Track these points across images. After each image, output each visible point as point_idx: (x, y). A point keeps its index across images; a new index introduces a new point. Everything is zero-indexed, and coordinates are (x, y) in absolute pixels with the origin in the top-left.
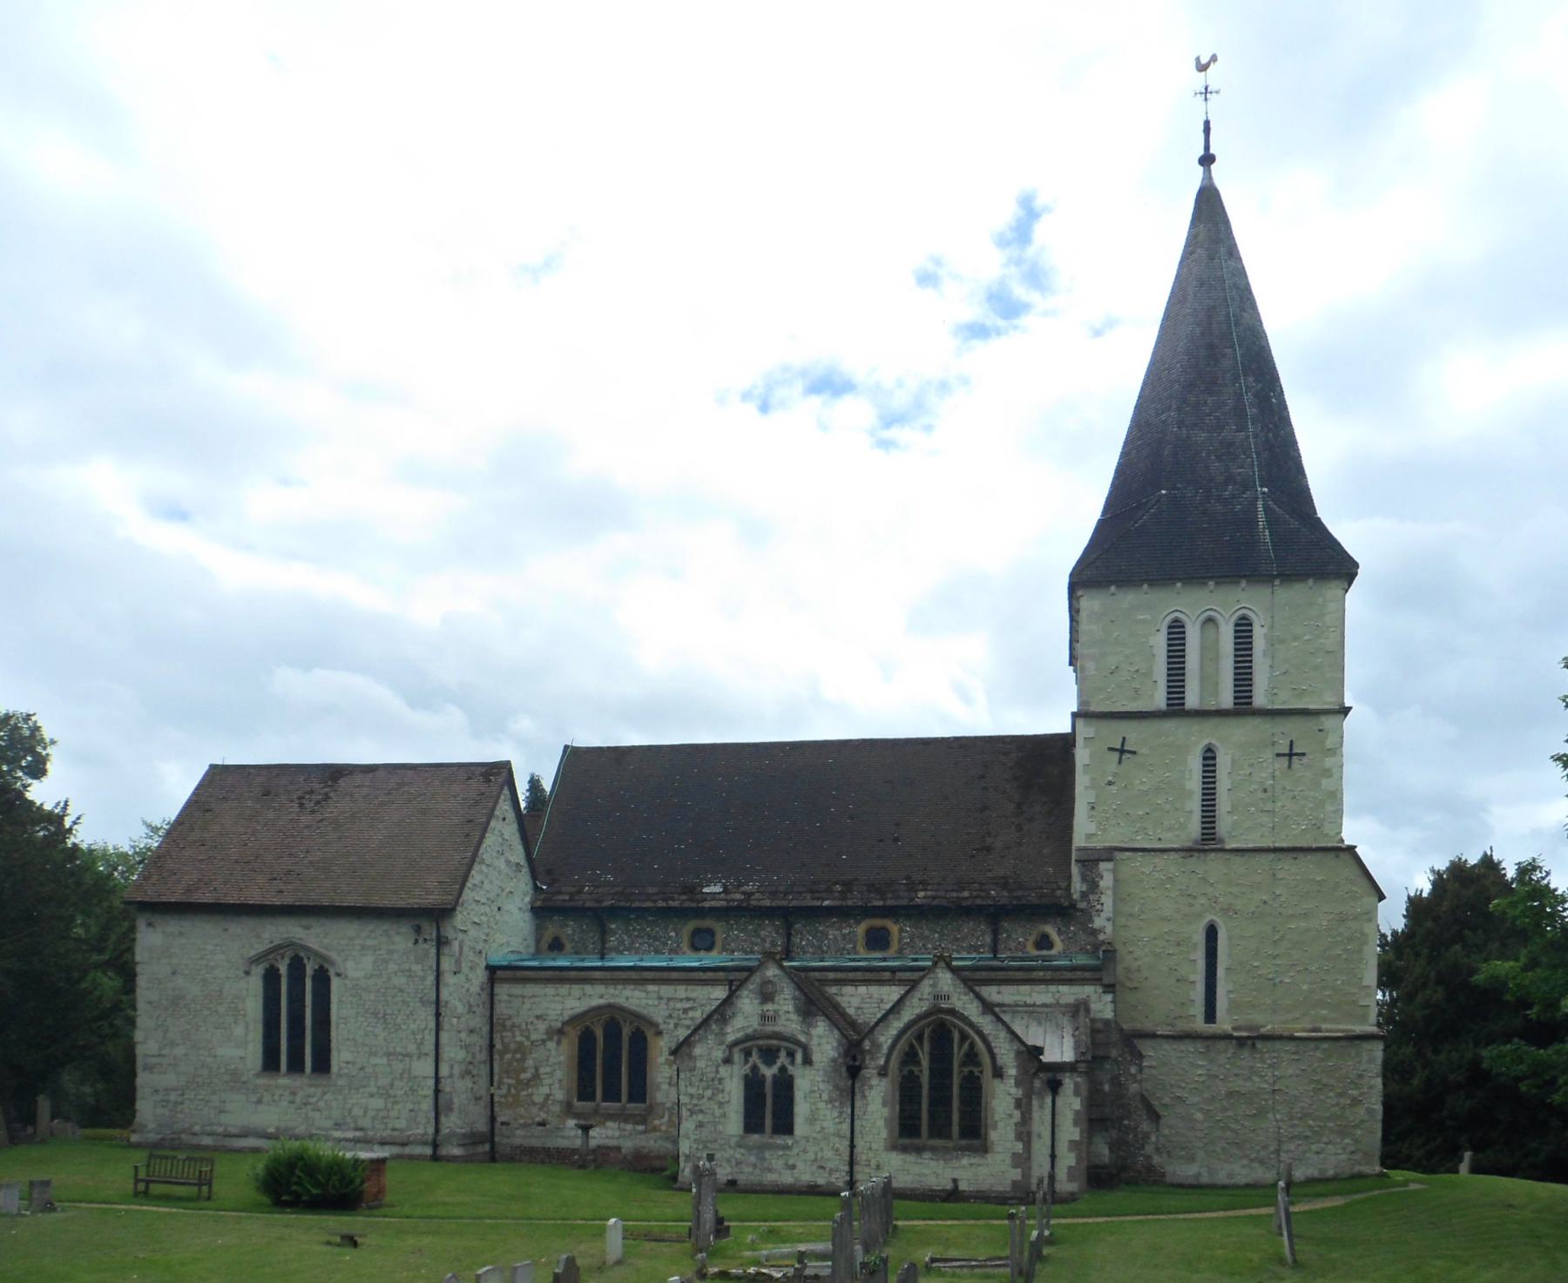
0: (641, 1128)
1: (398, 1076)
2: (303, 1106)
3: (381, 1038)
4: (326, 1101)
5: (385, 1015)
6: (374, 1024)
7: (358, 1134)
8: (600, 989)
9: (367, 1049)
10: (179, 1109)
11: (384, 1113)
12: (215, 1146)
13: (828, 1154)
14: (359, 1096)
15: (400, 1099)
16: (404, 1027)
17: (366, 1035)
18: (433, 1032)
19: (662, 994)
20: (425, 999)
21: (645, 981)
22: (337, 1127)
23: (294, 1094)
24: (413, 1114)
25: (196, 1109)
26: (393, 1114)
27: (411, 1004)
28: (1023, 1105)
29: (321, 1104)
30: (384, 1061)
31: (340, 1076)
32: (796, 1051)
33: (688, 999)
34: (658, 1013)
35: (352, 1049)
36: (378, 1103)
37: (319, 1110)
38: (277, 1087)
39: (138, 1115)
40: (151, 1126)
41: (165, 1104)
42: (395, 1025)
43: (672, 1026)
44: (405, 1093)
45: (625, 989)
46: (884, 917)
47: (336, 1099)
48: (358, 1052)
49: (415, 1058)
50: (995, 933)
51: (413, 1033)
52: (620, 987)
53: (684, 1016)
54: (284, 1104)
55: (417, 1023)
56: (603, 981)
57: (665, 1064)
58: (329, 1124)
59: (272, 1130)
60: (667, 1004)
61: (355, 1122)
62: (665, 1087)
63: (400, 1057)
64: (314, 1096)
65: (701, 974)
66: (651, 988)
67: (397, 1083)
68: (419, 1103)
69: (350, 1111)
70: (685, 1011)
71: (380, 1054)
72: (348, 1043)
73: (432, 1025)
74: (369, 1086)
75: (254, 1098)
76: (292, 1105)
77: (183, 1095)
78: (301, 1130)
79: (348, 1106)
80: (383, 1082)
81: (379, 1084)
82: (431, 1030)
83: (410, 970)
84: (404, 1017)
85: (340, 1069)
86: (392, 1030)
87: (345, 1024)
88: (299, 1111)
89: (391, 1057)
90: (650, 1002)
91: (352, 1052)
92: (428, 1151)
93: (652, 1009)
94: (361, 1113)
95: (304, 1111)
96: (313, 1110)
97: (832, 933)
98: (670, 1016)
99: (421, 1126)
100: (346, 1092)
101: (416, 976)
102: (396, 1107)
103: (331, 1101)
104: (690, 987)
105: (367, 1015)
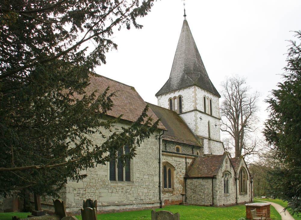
0: (172, 194)
2: (125, 193)
3: (146, 169)
4: (132, 191)
5: (147, 162)
8: (165, 157)
9: (143, 173)
10: (84, 197)
11: (147, 194)
13: (233, 197)
14: (141, 188)
15: (151, 189)
16: (151, 166)
17: (142, 168)
18: (158, 168)
19: (175, 160)
20: (156, 157)
21: (173, 156)
22: (136, 200)
23: (123, 189)
25: (90, 196)
26: (149, 194)
27: (153, 159)
28: (249, 185)
29: (131, 192)
30: (147, 177)
31: (136, 182)
32: (229, 174)
33: (179, 161)
34: (174, 164)
35: (139, 173)
37: (130, 194)
38: (118, 186)
40: (74, 204)
41: (78, 194)
42: (150, 165)
46: (179, 145)
47: (135, 190)
49: (154, 176)
50: (193, 151)
51: (154, 168)
52: (168, 157)
53: (179, 166)
54: (120, 193)
55: (155, 165)
56: (166, 155)
58: (133, 199)
59: (116, 202)
61: (140, 198)
62: (176, 183)
64: (129, 189)
66: (173, 158)
67: (151, 184)
68: (155, 190)
69: (139, 194)
70: (179, 164)
72: (138, 171)
73: (158, 166)
74: (143, 185)
75: (110, 191)
79: (138, 192)
80: (147, 184)
81: (146, 185)
83: (152, 148)
88: (124, 195)
90: (173, 161)
92: (159, 205)
93: (173, 163)
96: (129, 194)
98: (177, 166)
99: (156, 197)
100: (138, 187)
101: (154, 150)
102: (150, 192)
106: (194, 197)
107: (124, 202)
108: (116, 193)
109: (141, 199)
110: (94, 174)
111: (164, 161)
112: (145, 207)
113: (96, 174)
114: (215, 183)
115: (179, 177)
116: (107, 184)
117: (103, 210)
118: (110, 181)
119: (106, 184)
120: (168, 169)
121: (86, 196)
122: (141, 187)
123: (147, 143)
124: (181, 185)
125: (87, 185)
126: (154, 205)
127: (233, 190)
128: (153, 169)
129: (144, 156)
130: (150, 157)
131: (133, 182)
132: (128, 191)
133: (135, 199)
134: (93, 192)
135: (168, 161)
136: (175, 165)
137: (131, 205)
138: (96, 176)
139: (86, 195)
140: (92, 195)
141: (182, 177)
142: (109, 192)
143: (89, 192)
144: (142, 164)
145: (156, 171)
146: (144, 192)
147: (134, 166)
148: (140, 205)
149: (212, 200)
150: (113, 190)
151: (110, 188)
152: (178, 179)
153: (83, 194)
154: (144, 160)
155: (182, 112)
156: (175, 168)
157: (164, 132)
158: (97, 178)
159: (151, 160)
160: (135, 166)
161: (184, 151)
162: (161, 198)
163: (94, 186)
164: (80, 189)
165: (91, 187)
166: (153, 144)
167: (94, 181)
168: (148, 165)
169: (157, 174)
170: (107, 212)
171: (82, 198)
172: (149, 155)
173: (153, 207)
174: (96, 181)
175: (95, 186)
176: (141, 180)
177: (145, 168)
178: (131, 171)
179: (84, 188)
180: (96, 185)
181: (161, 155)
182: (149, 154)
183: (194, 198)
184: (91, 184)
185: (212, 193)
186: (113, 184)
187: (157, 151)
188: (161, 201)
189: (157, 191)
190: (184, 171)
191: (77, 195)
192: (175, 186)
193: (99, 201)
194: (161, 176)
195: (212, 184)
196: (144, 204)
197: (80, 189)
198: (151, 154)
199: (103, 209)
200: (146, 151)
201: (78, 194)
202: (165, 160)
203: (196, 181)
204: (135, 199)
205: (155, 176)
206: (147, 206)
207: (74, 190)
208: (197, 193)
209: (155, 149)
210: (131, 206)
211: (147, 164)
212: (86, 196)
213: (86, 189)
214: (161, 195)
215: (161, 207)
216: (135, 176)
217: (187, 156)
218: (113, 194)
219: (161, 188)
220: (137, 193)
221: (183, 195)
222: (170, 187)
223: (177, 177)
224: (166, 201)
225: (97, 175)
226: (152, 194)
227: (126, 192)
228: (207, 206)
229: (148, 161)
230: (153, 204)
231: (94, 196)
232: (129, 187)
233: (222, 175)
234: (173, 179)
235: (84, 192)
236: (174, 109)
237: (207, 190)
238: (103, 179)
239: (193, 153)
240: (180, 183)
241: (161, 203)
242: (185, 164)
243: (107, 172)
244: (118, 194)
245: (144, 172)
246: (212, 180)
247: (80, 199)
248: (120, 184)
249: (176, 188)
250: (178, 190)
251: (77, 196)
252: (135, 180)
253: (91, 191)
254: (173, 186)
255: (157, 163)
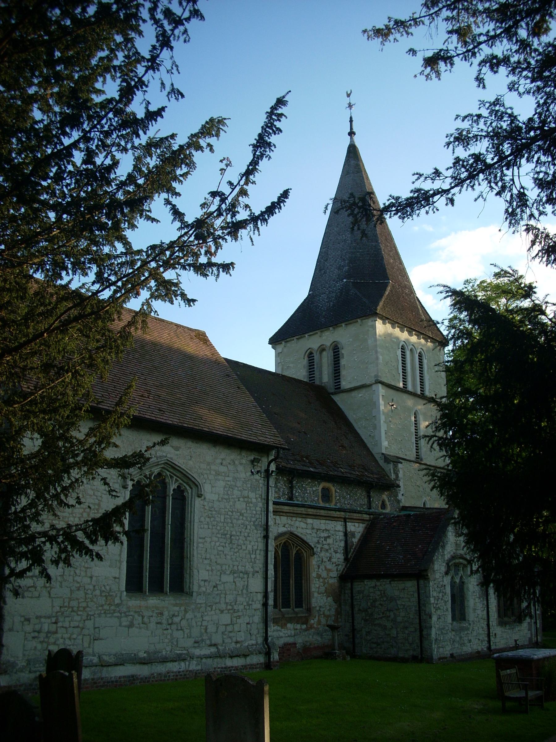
1: (240, 592)
2: (168, 627)
3: (228, 557)
4: (187, 620)
5: (231, 536)
6: (223, 544)
7: (213, 650)
8: (284, 519)
9: (219, 567)
10: (52, 640)
11: (230, 628)
12: (93, 679)
14: (213, 612)
15: (240, 614)
16: (244, 547)
18: (262, 553)
21: (308, 515)
22: (196, 645)
23: (161, 614)
24: (249, 626)
25: (70, 639)
26: (236, 628)
27: (249, 527)
29: (184, 623)
30: (230, 578)
31: (199, 594)
33: (326, 530)
34: (311, 539)
36: (226, 618)
37: (181, 630)
38: (147, 608)
39: (4, 651)
40: (21, 663)
41: (36, 634)
43: (319, 550)
44: (245, 609)
45: (296, 520)
47: (195, 616)
48: (212, 570)
49: (251, 575)
50: (369, 497)
51: (250, 553)
52: (294, 519)
53: (325, 542)
54: (152, 626)
55: (253, 543)
56: (286, 514)
57: (317, 577)
58: (189, 643)
59: (142, 655)
60: (316, 533)
61: (210, 639)
63: (241, 575)
65: (334, 512)
66: (310, 521)
67: (240, 599)
68: (253, 616)
69: (206, 629)
70: (326, 538)
71: (228, 572)
72: (206, 562)
73: (261, 546)
74: (220, 602)
75: (125, 621)
76: (158, 625)
77: (56, 623)
78: (166, 650)
79: (205, 623)
80: (230, 598)
81: (227, 601)
82: (261, 550)
83: (248, 497)
84: (244, 539)
85: (200, 586)
86: (236, 550)
87: (203, 543)
88: (165, 632)
89: (235, 575)
90: (309, 531)
91: (208, 570)
93: (308, 536)
94: (214, 630)
95: (169, 631)
96: (177, 630)
97: (309, 489)
99: (254, 637)
101: (251, 503)
103: (192, 619)
104: (327, 522)
105: (219, 536)
106: (368, 633)
107: (164, 653)
108: (140, 628)
109: (213, 642)
110: (83, 574)
111: (282, 530)
112: (223, 666)
113: (89, 575)
114: (425, 592)
115: (324, 574)
116: (117, 601)
117: (102, 679)
118: (125, 593)
119: (114, 601)
120: (294, 552)
121: (57, 639)
122: (214, 608)
123: (232, 483)
124: (330, 599)
125: (61, 607)
126: (248, 659)
127: (479, 612)
128: (248, 556)
129: (222, 520)
130: (240, 522)
131: (190, 594)
132: (176, 620)
133: (196, 642)
134: (78, 627)
135: (294, 530)
136: (316, 540)
137: (184, 660)
138: (89, 579)
139: (59, 635)
140: (74, 636)
141: (334, 574)
142: (120, 625)
143: (66, 628)
144: (218, 544)
145: (257, 561)
146: (220, 623)
147: (195, 548)
148: (209, 659)
149: (418, 641)
150: (133, 619)
151: (125, 613)
152: (321, 580)
153: (48, 632)
154: (222, 531)
155: (342, 388)
156: (315, 550)
157: (278, 452)
158: (91, 587)
159: (243, 530)
160: (197, 548)
161: (344, 498)
162: (270, 639)
163: (82, 609)
164: (41, 617)
165: (73, 611)
166: (249, 485)
167: (81, 594)
168: (235, 546)
169: (257, 569)
170: (112, 682)
171: (45, 645)
172: (237, 517)
173: (245, 667)
174: (86, 594)
175: (84, 608)
176: (214, 587)
177: (225, 555)
178: (187, 565)
179: (54, 614)
180: (88, 606)
181: (271, 515)
182: (239, 514)
183: (369, 638)
184: (74, 604)
185: (417, 621)
186: (135, 602)
187: (260, 505)
188: (269, 648)
189: (258, 618)
190: (339, 557)
191: (33, 635)
192: (313, 601)
193: (93, 652)
194: (269, 576)
195: (416, 595)
196: (220, 657)
197: (43, 620)
198: (242, 514)
199: (103, 676)
200: (228, 507)
201: (36, 634)
202: (284, 526)
203: (374, 587)
204: (195, 642)
205: (253, 575)
206: (229, 663)
207: (26, 623)
208: (377, 622)
209: (254, 500)
210: (183, 664)
211: (231, 543)
212: (57, 639)
213: (57, 619)
214: (269, 629)
215: (268, 666)
216: (195, 577)
217: (348, 515)
218: (134, 630)
219: (270, 609)
220: (201, 625)
221: (333, 628)
222: (299, 604)
223: (319, 576)
224: (286, 649)
225: (91, 577)
226: (244, 626)
227: (169, 624)
228: (404, 660)
229: (234, 533)
230: (245, 656)
231: (81, 637)
232: (177, 608)
233: (443, 569)
234: (308, 580)
235: (53, 628)
236: (321, 378)
237: (403, 614)
238: (108, 588)
239: (370, 502)
240: (328, 593)
241: (268, 654)
242: (342, 538)
243: (120, 568)
244: (147, 628)
245: (221, 565)
246: (415, 582)
247: (39, 647)
248: (153, 601)
249: (318, 608)
250: (322, 613)
251: (34, 638)
252: (195, 588)
253: (72, 625)
254: (309, 603)
255: (259, 540)
